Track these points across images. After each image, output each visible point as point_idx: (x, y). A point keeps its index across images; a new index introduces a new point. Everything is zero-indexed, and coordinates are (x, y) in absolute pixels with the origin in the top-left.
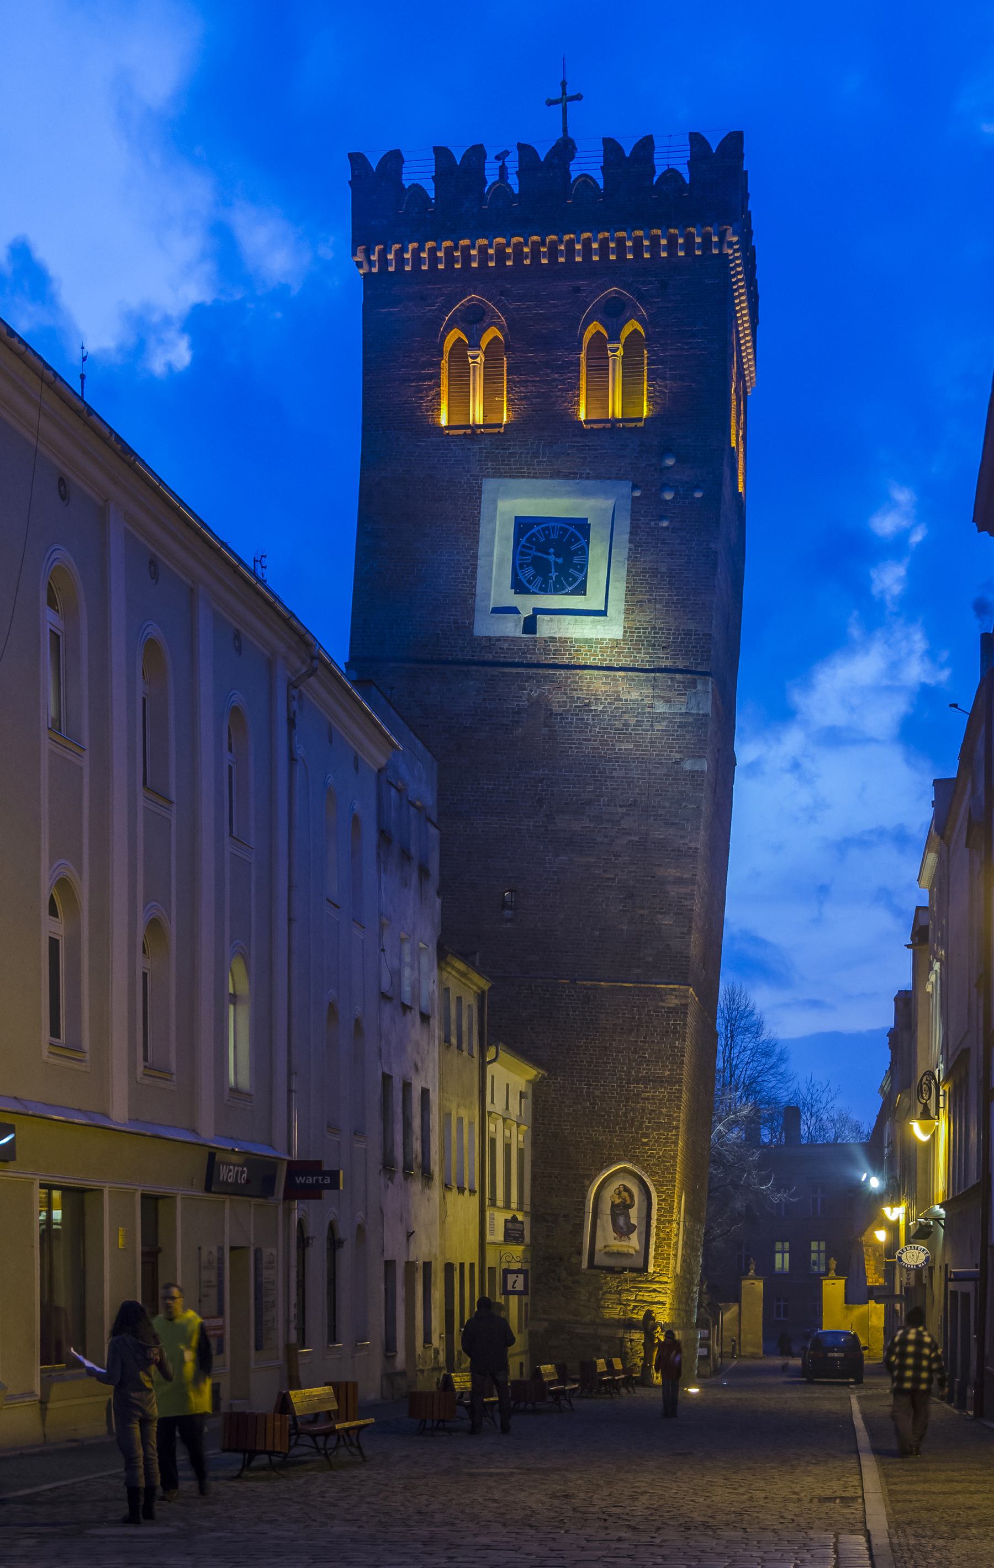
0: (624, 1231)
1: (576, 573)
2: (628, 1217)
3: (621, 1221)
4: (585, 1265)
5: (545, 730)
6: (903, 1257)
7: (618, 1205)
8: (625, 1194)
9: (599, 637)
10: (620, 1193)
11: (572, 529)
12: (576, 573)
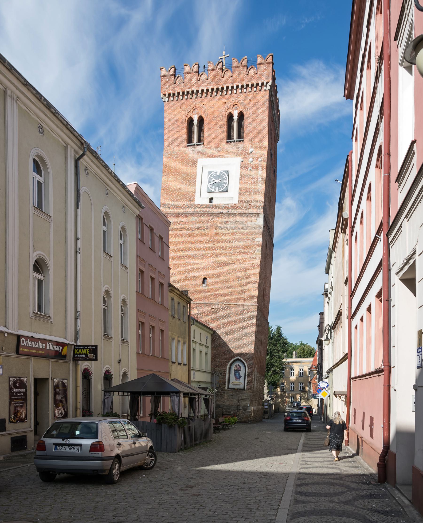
0: (238, 378)
1: (224, 185)
2: (239, 373)
3: (237, 375)
4: (226, 388)
5: (215, 231)
6: (320, 385)
8: (238, 367)
9: (231, 203)
11: (223, 172)
12: (224, 185)
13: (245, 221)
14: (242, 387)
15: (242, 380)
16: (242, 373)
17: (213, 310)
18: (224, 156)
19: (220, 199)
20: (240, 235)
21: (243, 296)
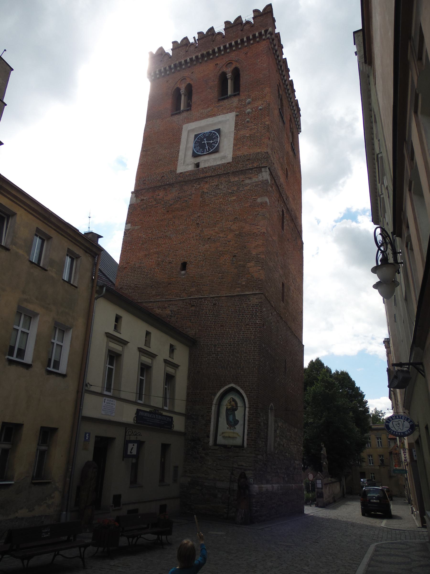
0: (233, 423)
3: (231, 418)
4: (211, 443)
5: (201, 199)
7: (230, 409)
8: (233, 403)
9: (223, 163)
10: (230, 402)
13: (241, 180)
14: (238, 442)
15: (239, 428)
16: (239, 414)
17: (193, 308)
18: (214, 115)
19: (208, 161)
20: (234, 198)
21: (239, 282)
